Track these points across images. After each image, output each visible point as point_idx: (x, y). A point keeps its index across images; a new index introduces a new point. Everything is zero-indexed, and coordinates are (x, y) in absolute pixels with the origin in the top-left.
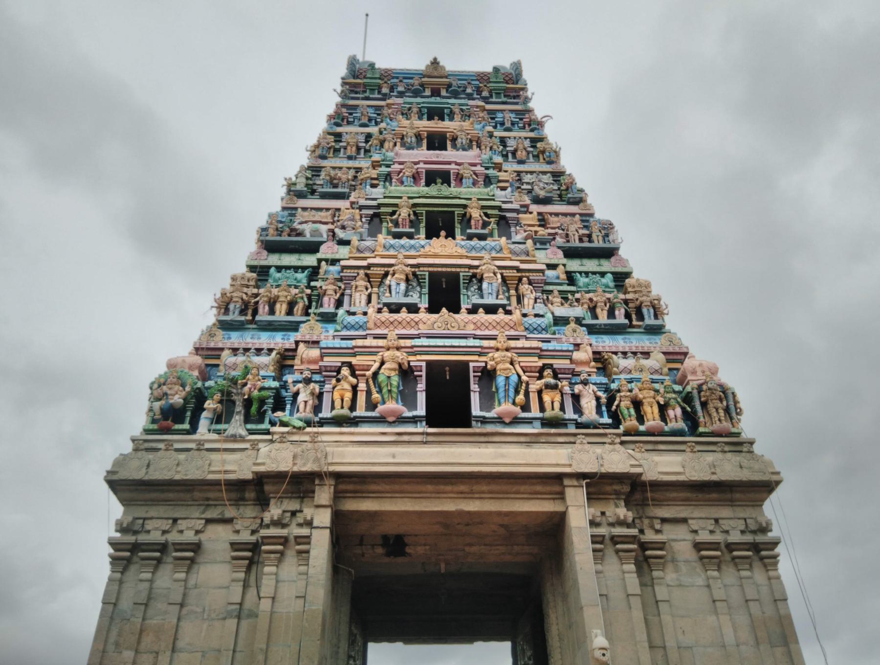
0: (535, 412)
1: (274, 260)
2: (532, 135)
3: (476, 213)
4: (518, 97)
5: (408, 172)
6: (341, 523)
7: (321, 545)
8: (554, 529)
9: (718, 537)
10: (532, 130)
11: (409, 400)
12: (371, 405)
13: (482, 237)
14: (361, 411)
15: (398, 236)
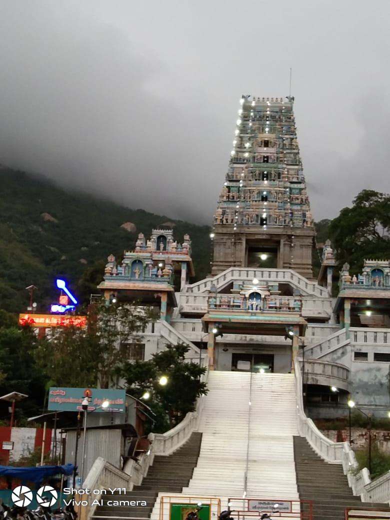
0: (278, 224)
1: (231, 184)
2: (291, 136)
3: (273, 172)
4: (290, 119)
5: (259, 157)
6: (247, 241)
7: (244, 242)
8: (278, 242)
9: (304, 244)
10: (292, 135)
11: (257, 221)
12: (251, 222)
13: (274, 180)
14: (250, 223)
15: (256, 180)
